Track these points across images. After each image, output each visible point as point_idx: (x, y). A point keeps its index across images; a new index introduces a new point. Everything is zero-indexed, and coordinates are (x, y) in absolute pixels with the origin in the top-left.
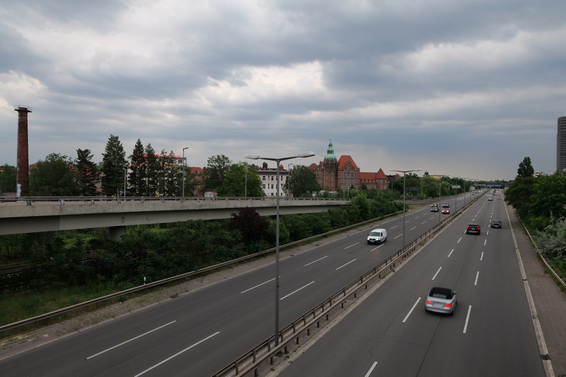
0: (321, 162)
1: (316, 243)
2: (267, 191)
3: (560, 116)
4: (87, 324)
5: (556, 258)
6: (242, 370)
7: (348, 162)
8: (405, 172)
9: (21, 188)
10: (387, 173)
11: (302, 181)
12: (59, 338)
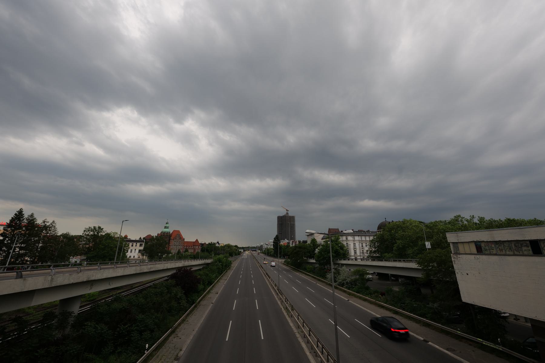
2: (129, 254)
7: (177, 235)
11: (155, 247)
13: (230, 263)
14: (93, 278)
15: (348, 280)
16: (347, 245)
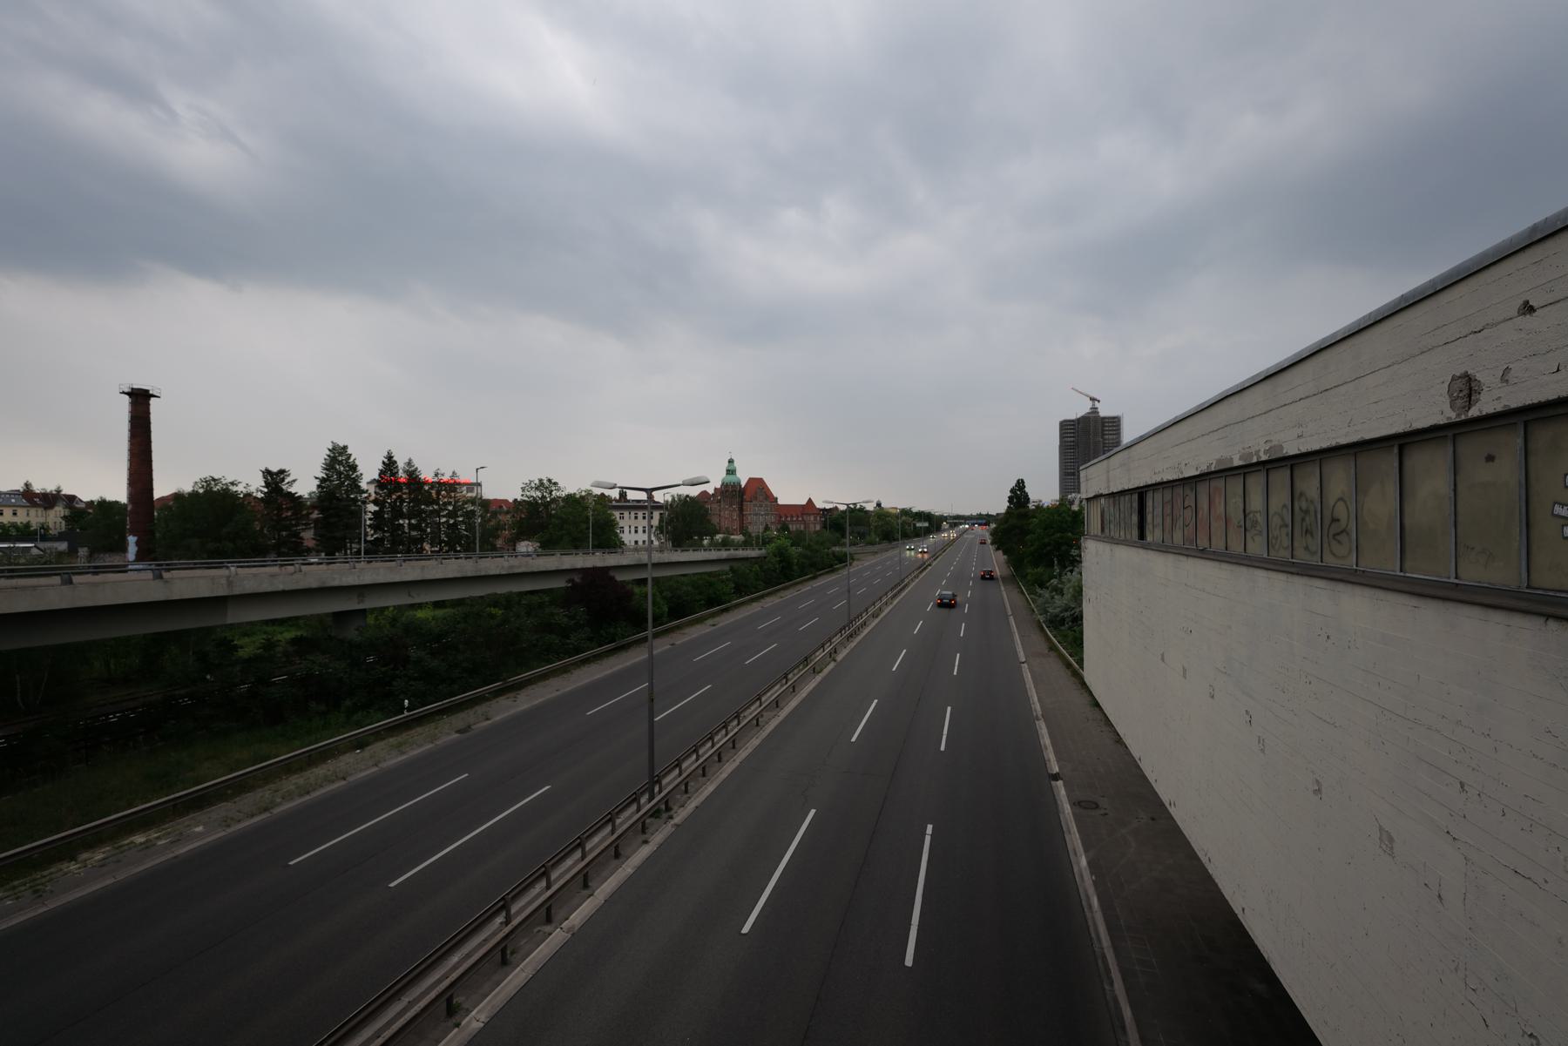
1: (710, 621)
2: (628, 538)
4: (288, 796)
6: (592, 850)
9: (137, 543)
10: (819, 504)
11: (686, 519)
12: (229, 830)
13: (842, 560)
14: (336, 583)
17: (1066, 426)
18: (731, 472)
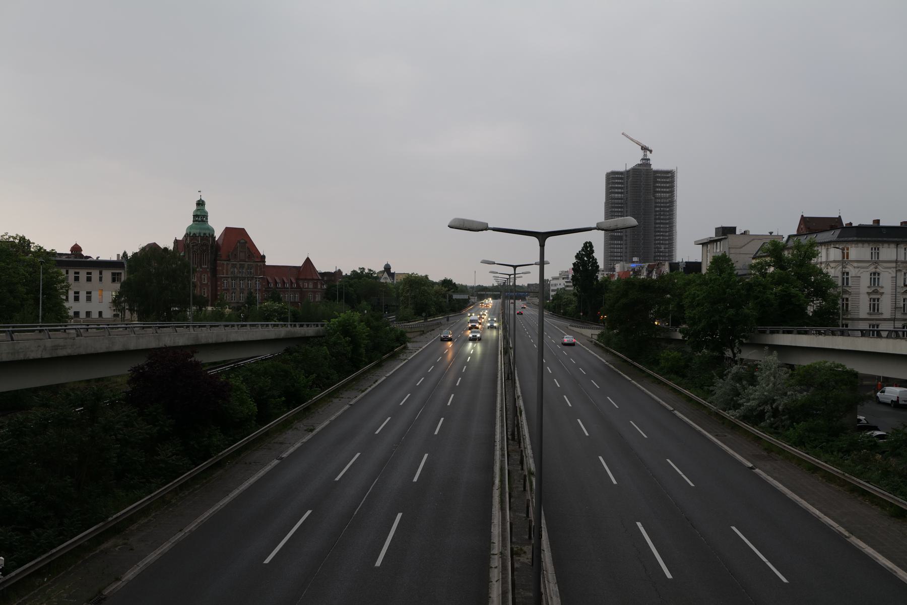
0: (176, 242)
3: (609, 171)
5: (762, 424)
8: (515, 267)
10: (322, 266)
13: (401, 340)
15: (782, 403)
16: (845, 281)
17: (613, 179)
18: (200, 216)
